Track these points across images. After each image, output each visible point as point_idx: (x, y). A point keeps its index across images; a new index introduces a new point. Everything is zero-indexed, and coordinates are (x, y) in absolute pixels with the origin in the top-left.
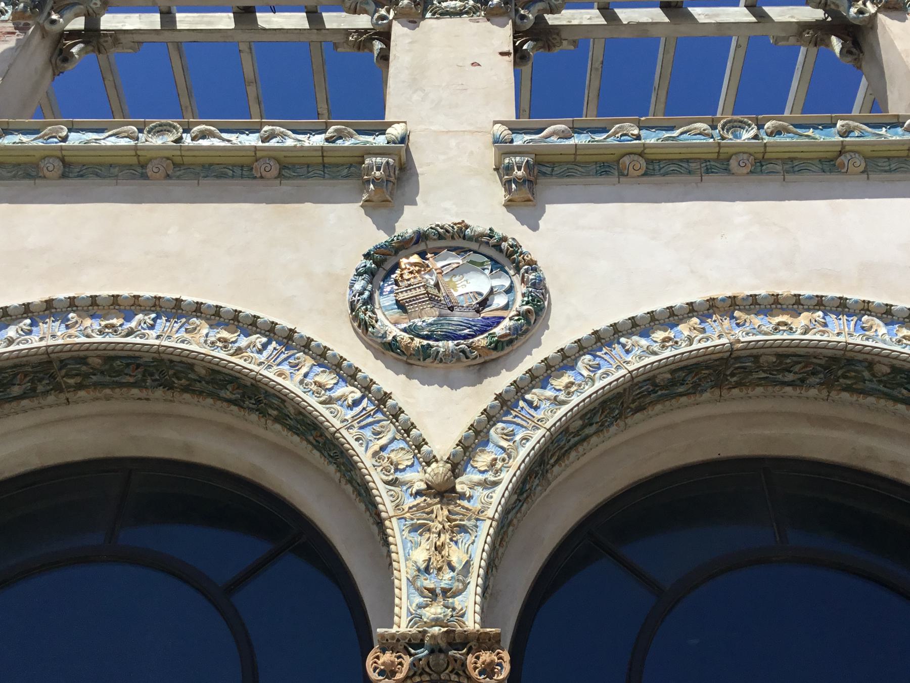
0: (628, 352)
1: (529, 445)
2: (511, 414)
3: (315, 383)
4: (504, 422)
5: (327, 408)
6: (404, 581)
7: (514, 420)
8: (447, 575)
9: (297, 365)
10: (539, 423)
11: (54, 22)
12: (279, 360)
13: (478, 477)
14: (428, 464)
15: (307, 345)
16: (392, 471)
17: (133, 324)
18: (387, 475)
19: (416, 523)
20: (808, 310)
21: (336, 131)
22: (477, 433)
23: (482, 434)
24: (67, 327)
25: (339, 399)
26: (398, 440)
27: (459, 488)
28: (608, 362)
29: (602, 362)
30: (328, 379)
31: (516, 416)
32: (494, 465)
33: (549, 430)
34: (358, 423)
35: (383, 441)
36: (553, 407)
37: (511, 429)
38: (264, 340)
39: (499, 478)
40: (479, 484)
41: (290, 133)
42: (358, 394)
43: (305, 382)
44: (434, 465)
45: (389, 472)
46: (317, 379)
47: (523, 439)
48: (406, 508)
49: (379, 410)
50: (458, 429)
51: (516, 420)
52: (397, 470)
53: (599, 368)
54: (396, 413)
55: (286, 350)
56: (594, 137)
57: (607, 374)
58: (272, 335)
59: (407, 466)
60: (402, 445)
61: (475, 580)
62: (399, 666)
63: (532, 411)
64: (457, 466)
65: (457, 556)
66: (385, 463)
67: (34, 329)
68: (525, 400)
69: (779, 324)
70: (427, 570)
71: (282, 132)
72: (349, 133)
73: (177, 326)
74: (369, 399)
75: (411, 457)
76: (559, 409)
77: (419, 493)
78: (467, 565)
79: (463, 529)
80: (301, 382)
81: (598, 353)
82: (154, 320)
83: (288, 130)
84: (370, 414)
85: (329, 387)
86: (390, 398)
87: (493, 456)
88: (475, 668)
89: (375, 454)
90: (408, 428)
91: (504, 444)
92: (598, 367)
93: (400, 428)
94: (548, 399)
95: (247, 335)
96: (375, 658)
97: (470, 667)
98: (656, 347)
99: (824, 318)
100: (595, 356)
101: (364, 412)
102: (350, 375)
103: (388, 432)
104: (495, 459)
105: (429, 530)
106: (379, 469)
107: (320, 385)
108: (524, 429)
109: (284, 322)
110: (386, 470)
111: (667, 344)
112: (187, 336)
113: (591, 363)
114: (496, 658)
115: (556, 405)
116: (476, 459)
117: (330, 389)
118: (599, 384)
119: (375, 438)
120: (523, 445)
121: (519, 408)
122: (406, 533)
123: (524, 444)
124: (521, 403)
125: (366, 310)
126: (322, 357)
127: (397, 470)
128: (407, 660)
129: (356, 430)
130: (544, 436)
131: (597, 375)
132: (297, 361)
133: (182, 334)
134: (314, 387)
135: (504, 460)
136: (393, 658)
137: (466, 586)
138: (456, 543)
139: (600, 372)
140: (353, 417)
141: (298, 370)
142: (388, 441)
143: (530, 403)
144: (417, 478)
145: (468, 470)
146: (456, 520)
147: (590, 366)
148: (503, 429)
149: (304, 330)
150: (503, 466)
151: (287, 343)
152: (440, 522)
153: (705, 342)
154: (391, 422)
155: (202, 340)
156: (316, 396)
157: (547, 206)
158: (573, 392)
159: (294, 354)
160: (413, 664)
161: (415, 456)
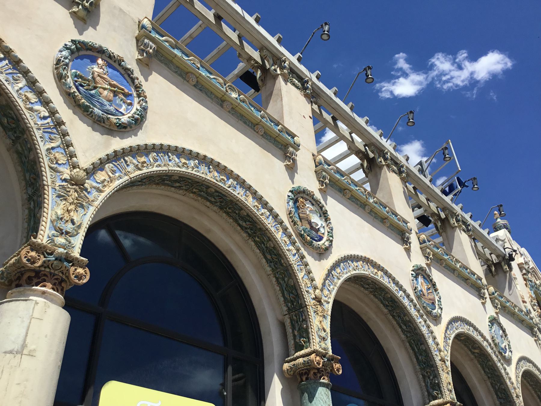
0: (170, 160)
1: (121, 181)
2: (117, 163)
3: (25, 96)
5: (29, 113)
7: (117, 166)
10: (128, 173)
12: (7, 72)
14: (74, 167)
15: (26, 73)
16: (55, 162)
18: (51, 163)
19: (60, 194)
20: (232, 178)
22: (101, 163)
23: (102, 164)
25: (36, 111)
26: (61, 148)
27: (86, 185)
28: (162, 161)
29: (159, 159)
31: (118, 164)
32: (104, 182)
34: (44, 129)
35: (53, 145)
39: (104, 189)
40: (94, 188)
42: (47, 114)
43: (20, 92)
45: (53, 162)
49: (55, 127)
50: (95, 159)
51: (118, 166)
54: (65, 134)
55: (13, 68)
57: (159, 166)
58: (7, 55)
59: (62, 163)
60: (63, 151)
61: (82, 233)
62: (38, 260)
66: (52, 156)
68: (124, 160)
74: (52, 119)
75: (66, 160)
76: (137, 171)
77: (65, 180)
79: (82, 206)
80: (18, 91)
81: (159, 155)
84: (50, 127)
86: (64, 125)
88: (73, 274)
89: (48, 150)
90: (69, 145)
93: (64, 142)
94: (134, 164)
96: (26, 252)
97: (71, 272)
98: (180, 164)
100: (158, 156)
101: (48, 125)
102: (46, 103)
103: (57, 141)
105: (65, 200)
106: (48, 158)
107: (27, 98)
108: (120, 172)
114: (84, 272)
115: (136, 168)
116: (96, 175)
117: (32, 103)
118: (155, 169)
119: (50, 141)
120: (118, 180)
121: (121, 162)
122: (54, 196)
123: (119, 179)
124: (122, 160)
126: (32, 83)
127: (57, 163)
128: (43, 259)
129: (41, 132)
130: (128, 180)
131: (155, 165)
132: (18, 78)
135: (108, 182)
136: (36, 255)
137: (78, 233)
138: (77, 211)
140: (41, 124)
141: (17, 83)
142: (56, 146)
144: (66, 172)
145: (91, 178)
146: (80, 200)
147: (154, 158)
148: (112, 168)
150: (107, 185)
151: (15, 65)
152: (72, 198)
154: (60, 137)
156: (24, 103)
158: (144, 167)
159: (17, 73)
160: (44, 262)
161: (68, 160)
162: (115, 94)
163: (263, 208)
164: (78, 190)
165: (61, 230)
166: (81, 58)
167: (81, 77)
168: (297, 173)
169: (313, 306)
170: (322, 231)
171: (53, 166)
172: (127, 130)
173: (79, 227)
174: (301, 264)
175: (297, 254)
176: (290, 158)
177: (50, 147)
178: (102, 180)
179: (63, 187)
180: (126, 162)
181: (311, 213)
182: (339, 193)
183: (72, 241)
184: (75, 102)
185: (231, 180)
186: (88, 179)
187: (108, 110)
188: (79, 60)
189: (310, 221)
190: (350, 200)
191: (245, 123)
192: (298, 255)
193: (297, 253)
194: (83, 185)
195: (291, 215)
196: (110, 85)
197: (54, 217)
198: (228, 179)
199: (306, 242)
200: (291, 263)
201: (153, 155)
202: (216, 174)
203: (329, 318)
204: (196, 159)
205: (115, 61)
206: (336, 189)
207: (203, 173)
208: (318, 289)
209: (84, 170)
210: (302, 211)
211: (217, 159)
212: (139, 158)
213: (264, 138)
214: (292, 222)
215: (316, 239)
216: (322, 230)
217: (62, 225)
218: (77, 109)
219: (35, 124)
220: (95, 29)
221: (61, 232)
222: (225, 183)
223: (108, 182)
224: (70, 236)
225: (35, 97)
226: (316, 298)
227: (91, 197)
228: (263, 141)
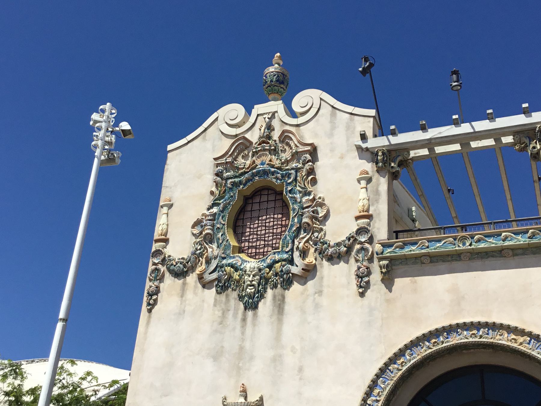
1: (389, 386)
4: (382, 377)
13: (374, 398)
31: (386, 375)
33: (395, 381)
37: (384, 380)
40: (374, 401)
47: (387, 384)
63: (390, 374)
68: (388, 369)
76: (399, 372)
87: (379, 391)
91: (383, 386)
92: (412, 355)
104: (379, 392)
111: (435, 344)
113: (410, 353)
115: (398, 371)
116: (374, 391)
124: (387, 371)
130: (394, 383)
135: (382, 392)
143: (390, 370)
150: (382, 394)
153: (447, 343)
158: (404, 366)
178: (377, 393)
180: (390, 370)
198: (478, 331)
201: (408, 352)
212: (398, 362)
222: (476, 336)
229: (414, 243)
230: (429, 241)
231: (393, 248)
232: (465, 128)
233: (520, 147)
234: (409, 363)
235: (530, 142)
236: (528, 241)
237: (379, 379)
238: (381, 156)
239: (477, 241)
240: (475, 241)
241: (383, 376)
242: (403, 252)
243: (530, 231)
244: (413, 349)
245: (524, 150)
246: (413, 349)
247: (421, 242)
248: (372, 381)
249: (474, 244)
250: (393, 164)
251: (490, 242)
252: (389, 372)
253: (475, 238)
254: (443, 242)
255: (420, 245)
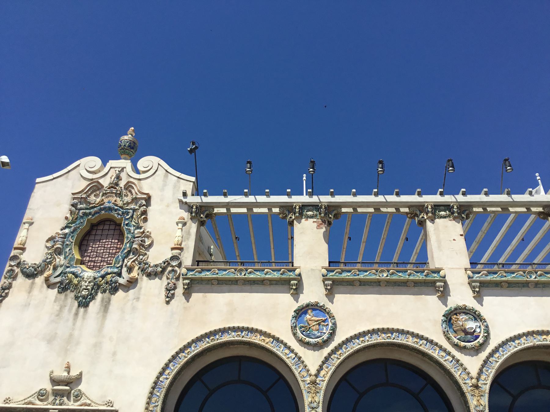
0: (354, 344)
6: (307, 405)
8: (315, 404)
9: (280, 347)
11: (201, 217)
14: (310, 376)
15: (282, 342)
17: (243, 334)
21: (283, 271)
24: (229, 335)
27: (317, 382)
30: (287, 351)
35: (300, 369)
36: (337, 360)
38: (272, 340)
41: (271, 271)
44: (312, 376)
46: (285, 352)
48: (306, 387)
49: (299, 361)
50: (317, 367)
52: (304, 377)
53: (347, 349)
56: (347, 274)
64: (317, 376)
65: (317, 400)
66: (301, 375)
67: (222, 335)
68: (331, 358)
69: (388, 336)
70: (311, 403)
71: (270, 271)
72: (286, 272)
73: (253, 335)
77: (309, 384)
78: (319, 401)
79: (318, 392)
80: (282, 352)
82: (248, 333)
83: (271, 270)
85: (288, 354)
95: (269, 338)
99: (398, 335)
102: (292, 351)
104: (324, 374)
105: (311, 393)
109: (277, 335)
110: (301, 377)
112: (255, 338)
120: (330, 370)
124: (330, 359)
125: (295, 329)
127: (304, 377)
129: (294, 366)
133: (254, 338)
134: (285, 354)
135: (326, 374)
137: (319, 406)
139: (347, 350)
143: (332, 359)
144: (308, 379)
149: (281, 338)
155: (258, 339)
157: (335, 295)
161: (307, 373)
162: (319, 324)
163: (421, 340)
164: (315, 386)
165: (312, 407)
166: (300, 316)
167: (303, 327)
168: (450, 296)
169: (470, 392)
170: (477, 331)
171: (303, 379)
172: (329, 341)
173: (319, 403)
174: (458, 365)
175: (453, 360)
176: (439, 290)
177: (299, 371)
178: (323, 375)
179: (309, 387)
180: (332, 359)
181: (465, 321)
182: (497, 288)
183: (318, 411)
184: (303, 342)
185: (394, 334)
186: (317, 378)
187: (318, 336)
188: (300, 318)
189: (465, 329)
190: (509, 287)
191: (399, 285)
192: (454, 360)
193: (453, 359)
194: (316, 382)
195: (445, 334)
196: (316, 321)
197: (308, 403)
199: (461, 348)
200: (448, 368)
202: (383, 335)
203: (487, 396)
204: (369, 334)
205: (315, 306)
206: (492, 287)
207: (375, 340)
208: (473, 378)
209: (314, 376)
210: (456, 325)
211: (381, 327)
213: (417, 286)
214: (447, 338)
215: (472, 340)
216: (478, 330)
217: (312, 405)
218: (306, 345)
219: (291, 364)
220: (303, 294)
221: (313, 408)
223: (326, 374)
224: (316, 409)
225: (288, 350)
226: (473, 385)
227: (320, 386)
228: (416, 289)
229: (349, 271)
230: (359, 271)
231: (335, 272)
232: (381, 198)
233: (410, 216)
234: (503, 357)
235: (420, 214)
236: (425, 278)
237: (483, 368)
238: (298, 209)
239: (539, 275)
240: (391, 274)
241: (485, 366)
242: (342, 277)
243: (426, 271)
244: (347, 344)
245: (413, 218)
246: (347, 344)
247: (353, 270)
248: (479, 369)
249: (538, 277)
250: (330, 216)
251: (400, 276)
252: (490, 363)
253: (538, 274)
254: (516, 274)
255: (499, 274)
